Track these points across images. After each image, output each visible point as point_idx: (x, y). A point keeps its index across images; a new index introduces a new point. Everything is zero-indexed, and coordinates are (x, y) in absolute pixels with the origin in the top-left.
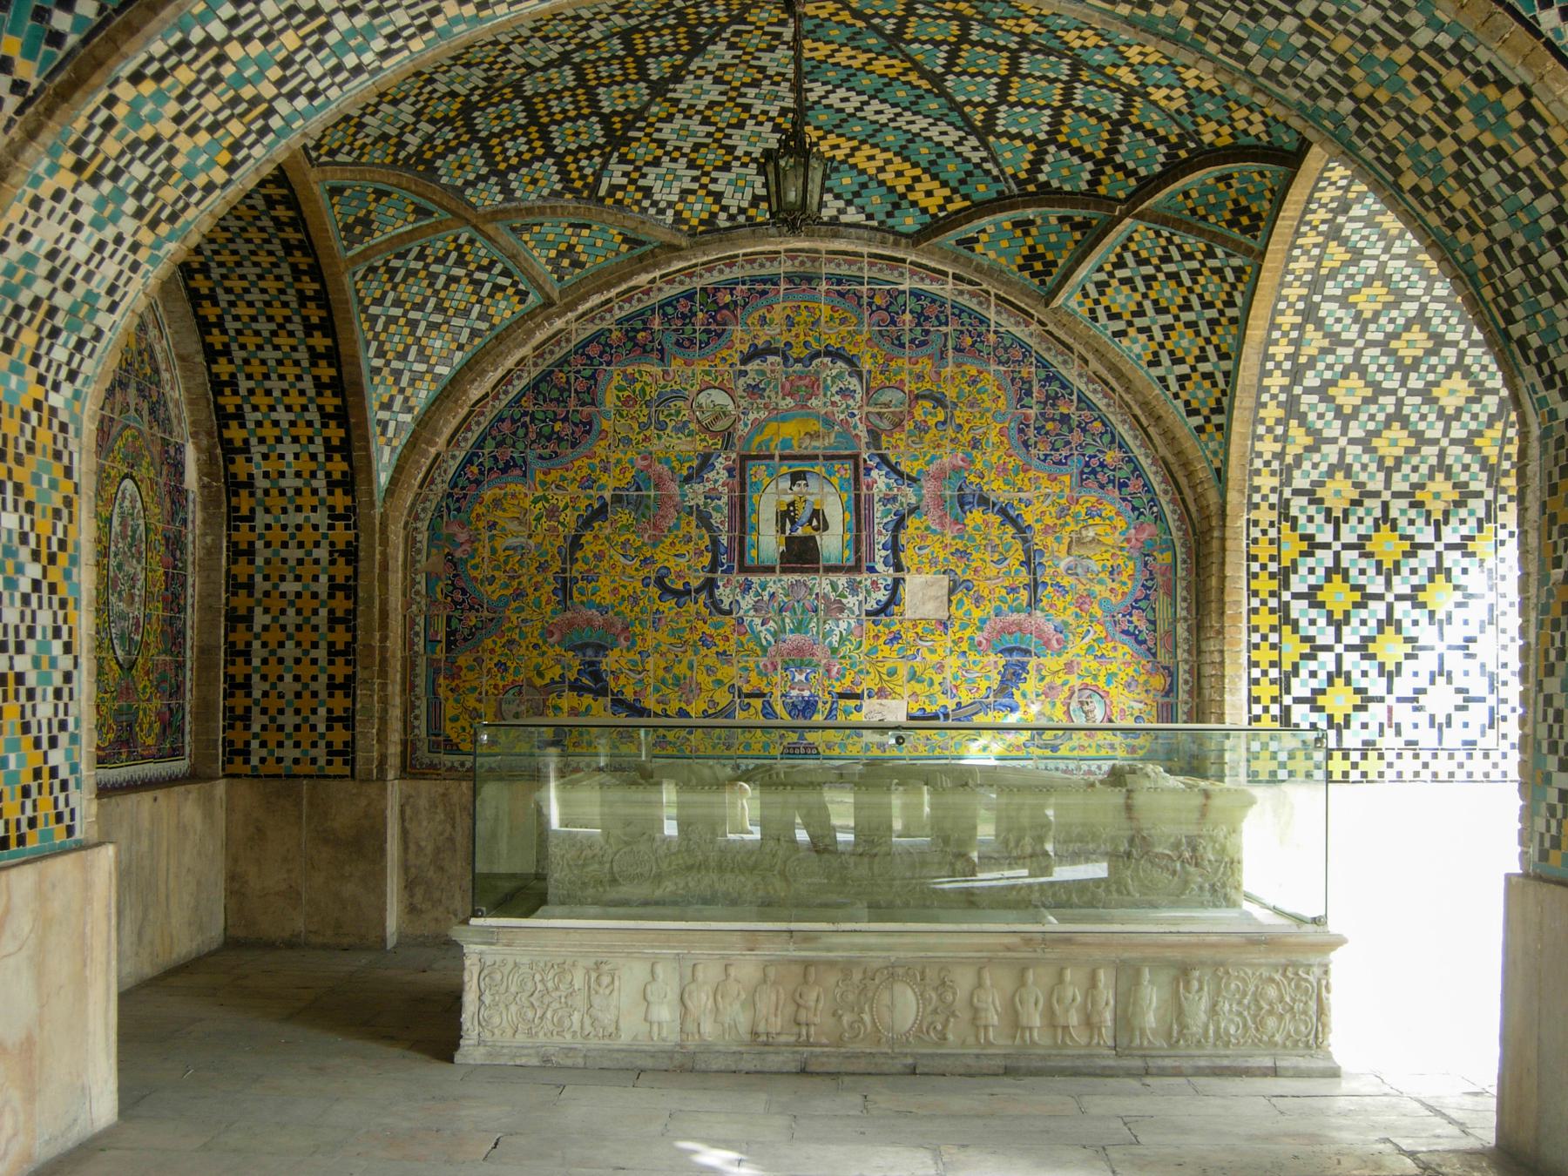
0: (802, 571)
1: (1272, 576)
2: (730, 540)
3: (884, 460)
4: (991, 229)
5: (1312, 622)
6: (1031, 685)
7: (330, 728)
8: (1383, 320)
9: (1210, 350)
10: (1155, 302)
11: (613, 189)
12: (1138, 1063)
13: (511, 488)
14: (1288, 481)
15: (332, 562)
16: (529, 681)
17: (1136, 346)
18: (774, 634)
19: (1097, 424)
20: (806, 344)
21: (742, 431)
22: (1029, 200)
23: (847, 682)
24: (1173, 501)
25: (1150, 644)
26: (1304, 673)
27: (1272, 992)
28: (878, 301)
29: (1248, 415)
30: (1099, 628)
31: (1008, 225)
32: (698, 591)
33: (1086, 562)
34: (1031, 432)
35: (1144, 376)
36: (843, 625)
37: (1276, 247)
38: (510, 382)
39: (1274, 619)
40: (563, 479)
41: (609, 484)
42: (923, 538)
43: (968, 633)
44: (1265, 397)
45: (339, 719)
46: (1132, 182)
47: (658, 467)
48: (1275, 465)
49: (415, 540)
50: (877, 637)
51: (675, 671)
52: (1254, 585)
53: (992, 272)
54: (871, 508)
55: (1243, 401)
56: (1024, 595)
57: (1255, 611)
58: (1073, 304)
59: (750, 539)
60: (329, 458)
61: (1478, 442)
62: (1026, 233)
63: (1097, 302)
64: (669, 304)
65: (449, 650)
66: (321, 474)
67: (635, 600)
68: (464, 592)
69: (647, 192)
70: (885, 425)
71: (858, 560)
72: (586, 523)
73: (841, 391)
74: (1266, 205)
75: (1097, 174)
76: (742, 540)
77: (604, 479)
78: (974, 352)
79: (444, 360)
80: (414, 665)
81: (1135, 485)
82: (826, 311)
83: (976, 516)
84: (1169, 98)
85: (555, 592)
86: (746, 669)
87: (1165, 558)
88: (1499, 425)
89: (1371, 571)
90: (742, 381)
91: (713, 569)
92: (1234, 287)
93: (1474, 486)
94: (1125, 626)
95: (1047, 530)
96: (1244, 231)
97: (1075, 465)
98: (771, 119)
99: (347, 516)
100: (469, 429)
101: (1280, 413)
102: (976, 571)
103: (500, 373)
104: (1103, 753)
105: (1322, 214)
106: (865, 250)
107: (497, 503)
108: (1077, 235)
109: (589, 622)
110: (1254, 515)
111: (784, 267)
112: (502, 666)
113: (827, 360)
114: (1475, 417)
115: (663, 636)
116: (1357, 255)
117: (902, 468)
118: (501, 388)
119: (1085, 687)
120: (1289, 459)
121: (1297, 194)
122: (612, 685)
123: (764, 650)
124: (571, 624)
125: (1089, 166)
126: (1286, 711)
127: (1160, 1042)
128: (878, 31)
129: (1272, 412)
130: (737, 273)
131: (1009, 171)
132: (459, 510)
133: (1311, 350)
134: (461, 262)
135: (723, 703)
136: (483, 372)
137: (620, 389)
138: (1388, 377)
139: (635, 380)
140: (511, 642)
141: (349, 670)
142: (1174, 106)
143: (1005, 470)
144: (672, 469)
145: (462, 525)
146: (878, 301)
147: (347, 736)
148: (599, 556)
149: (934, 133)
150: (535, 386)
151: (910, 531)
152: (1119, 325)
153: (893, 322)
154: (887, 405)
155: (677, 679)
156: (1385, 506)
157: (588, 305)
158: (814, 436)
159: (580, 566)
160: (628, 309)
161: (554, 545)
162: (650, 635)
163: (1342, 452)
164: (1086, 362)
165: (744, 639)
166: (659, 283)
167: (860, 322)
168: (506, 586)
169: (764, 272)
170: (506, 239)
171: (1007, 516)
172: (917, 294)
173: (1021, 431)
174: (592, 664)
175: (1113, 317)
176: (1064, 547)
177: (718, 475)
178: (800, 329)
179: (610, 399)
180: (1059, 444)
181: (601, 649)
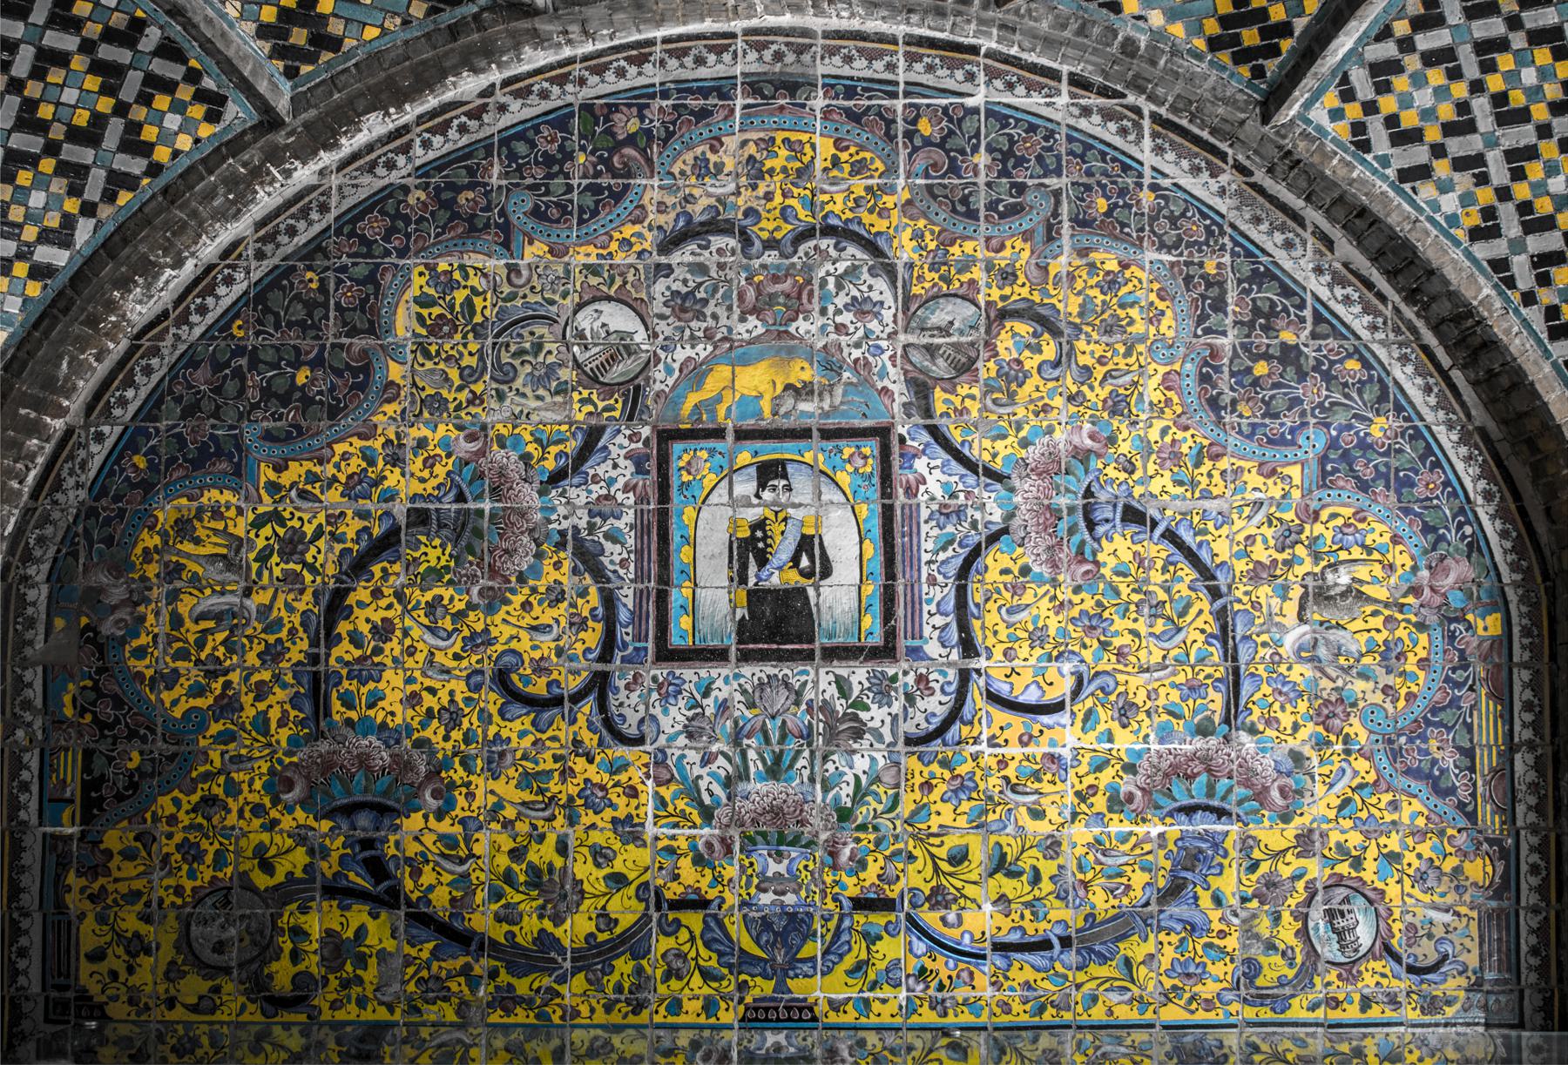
2: (640, 596)
13: (214, 495)
16: (244, 880)
18: (728, 783)
19: (1353, 365)
20: (785, 213)
21: (661, 379)
24: (1500, 514)
25: (1463, 794)
28: (925, 127)
30: (1362, 765)
32: (577, 698)
33: (1334, 635)
34: (1224, 382)
36: (861, 764)
38: (210, 290)
40: (312, 478)
41: (405, 484)
42: (1017, 590)
43: (1106, 777)
47: (498, 454)
49: (22, 601)
50: (927, 786)
51: (532, 857)
54: (913, 532)
56: (1216, 701)
59: (679, 595)
64: (520, 136)
65: (87, 819)
67: (452, 716)
68: (118, 703)
70: (941, 368)
71: (890, 635)
72: (358, 567)
76: (662, 598)
77: (393, 478)
78: (1114, 226)
81: (1426, 483)
82: (825, 148)
83: (1118, 548)
85: (295, 701)
86: (671, 851)
87: (1490, 625)
90: (660, 287)
91: (606, 654)
94: (1413, 760)
95: (1259, 573)
97: (1314, 441)
100: (129, 382)
102: (1120, 654)
104: (1375, 1013)
106: (900, 30)
107: (184, 528)
109: (363, 760)
111: (748, 64)
112: (191, 853)
113: (826, 243)
115: (507, 788)
117: (974, 453)
118: (194, 302)
119: (1338, 881)
122: (409, 884)
123: (707, 814)
124: (327, 765)
130: (652, 75)
132: (109, 541)
135: (627, 921)
136: (149, 270)
139: (451, 285)
140: (209, 801)
143: (1176, 457)
144: (527, 458)
148: (383, 631)
150: (259, 299)
151: (993, 575)
153: (954, 170)
154: (944, 331)
155: (534, 870)
157: (361, 139)
158: (801, 391)
159: (344, 650)
162: (480, 783)
164: (1329, 244)
165: (666, 793)
166: (500, 97)
167: (891, 170)
168: (198, 691)
169: (703, 72)
172: (998, 116)
173: (1204, 379)
174: (367, 844)
176: (1291, 608)
178: (775, 184)
179: (404, 323)
180: (1279, 404)
181: (385, 812)
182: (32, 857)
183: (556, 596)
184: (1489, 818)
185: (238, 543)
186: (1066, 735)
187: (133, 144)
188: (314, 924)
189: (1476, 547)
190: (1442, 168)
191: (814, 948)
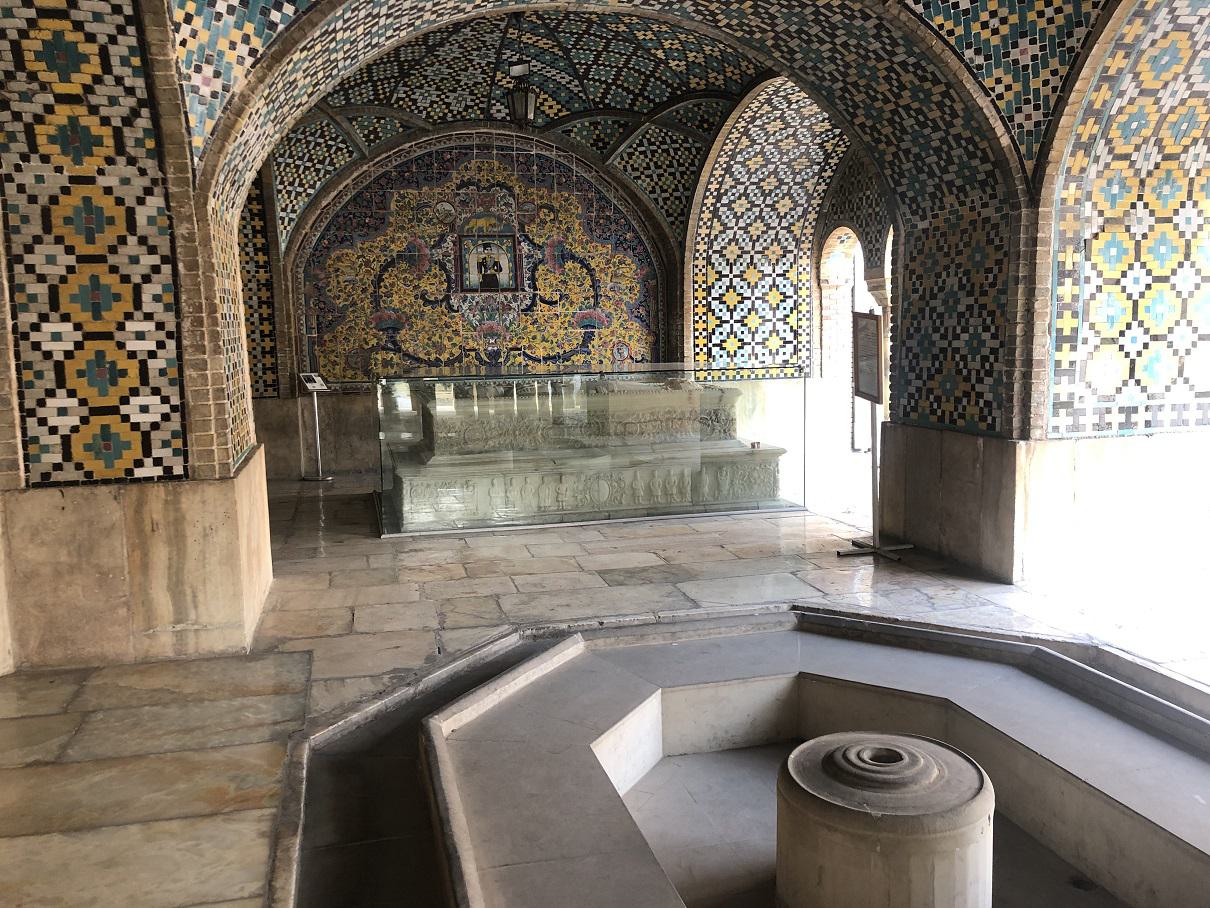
0: (491, 291)
1: (704, 290)
3: (527, 237)
4: (579, 126)
5: (721, 310)
6: (596, 342)
7: (264, 373)
8: (759, 173)
9: (680, 187)
10: (656, 163)
11: (399, 99)
12: (702, 508)
14: (711, 247)
15: (259, 290)
16: (361, 347)
17: (644, 183)
21: (459, 223)
22: (600, 112)
23: (514, 343)
24: (656, 256)
26: (717, 333)
27: (756, 475)
28: (521, 159)
29: (697, 217)
31: (587, 124)
32: (442, 301)
35: (644, 198)
36: (511, 316)
37: (720, 138)
39: (705, 310)
44: (704, 208)
45: (269, 369)
46: (652, 105)
48: (706, 239)
52: (696, 294)
53: (574, 147)
55: (695, 210)
56: (592, 301)
57: (697, 306)
58: (616, 163)
60: (255, 237)
61: (792, 228)
62: (596, 128)
63: (627, 162)
66: (250, 245)
69: (415, 101)
70: (526, 220)
72: (384, 269)
73: (505, 204)
74: (717, 119)
75: (634, 101)
76: (462, 277)
77: (393, 246)
79: (312, 187)
80: (301, 340)
82: (496, 163)
83: (569, 264)
84: (678, 65)
87: (653, 282)
88: (802, 220)
89: (746, 287)
92: (695, 157)
93: (789, 248)
95: (602, 270)
96: (704, 130)
97: (613, 241)
98: (481, 67)
99: (266, 266)
100: (322, 221)
101: (710, 216)
103: (335, 193)
105: (743, 124)
107: (339, 259)
108: (621, 130)
110: (696, 262)
111: (477, 141)
114: (792, 217)
115: (426, 323)
116: (753, 142)
120: (712, 237)
121: (735, 114)
125: (631, 96)
126: (710, 350)
127: (710, 498)
128: (547, 26)
129: (707, 215)
131: (591, 97)
133: (725, 187)
134: (322, 136)
137: (397, 201)
138: (758, 199)
141: (272, 344)
142: (679, 69)
145: (321, 270)
146: (521, 159)
147: (274, 377)
148: (392, 285)
149: (558, 78)
150: (354, 199)
152: (638, 174)
156: (752, 257)
159: (383, 290)
160: (399, 161)
161: (369, 279)
163: (735, 233)
168: (346, 300)
170: (345, 125)
171: (584, 264)
175: (634, 169)
177: (449, 244)
179: (393, 206)
181: (396, 330)
182: (305, 341)
183: (435, 276)
184: (653, 327)
185: (354, 263)
186: (559, 309)
187: (332, 163)
188: (379, 357)
189: (650, 264)
190: (643, 177)
191: (501, 360)
